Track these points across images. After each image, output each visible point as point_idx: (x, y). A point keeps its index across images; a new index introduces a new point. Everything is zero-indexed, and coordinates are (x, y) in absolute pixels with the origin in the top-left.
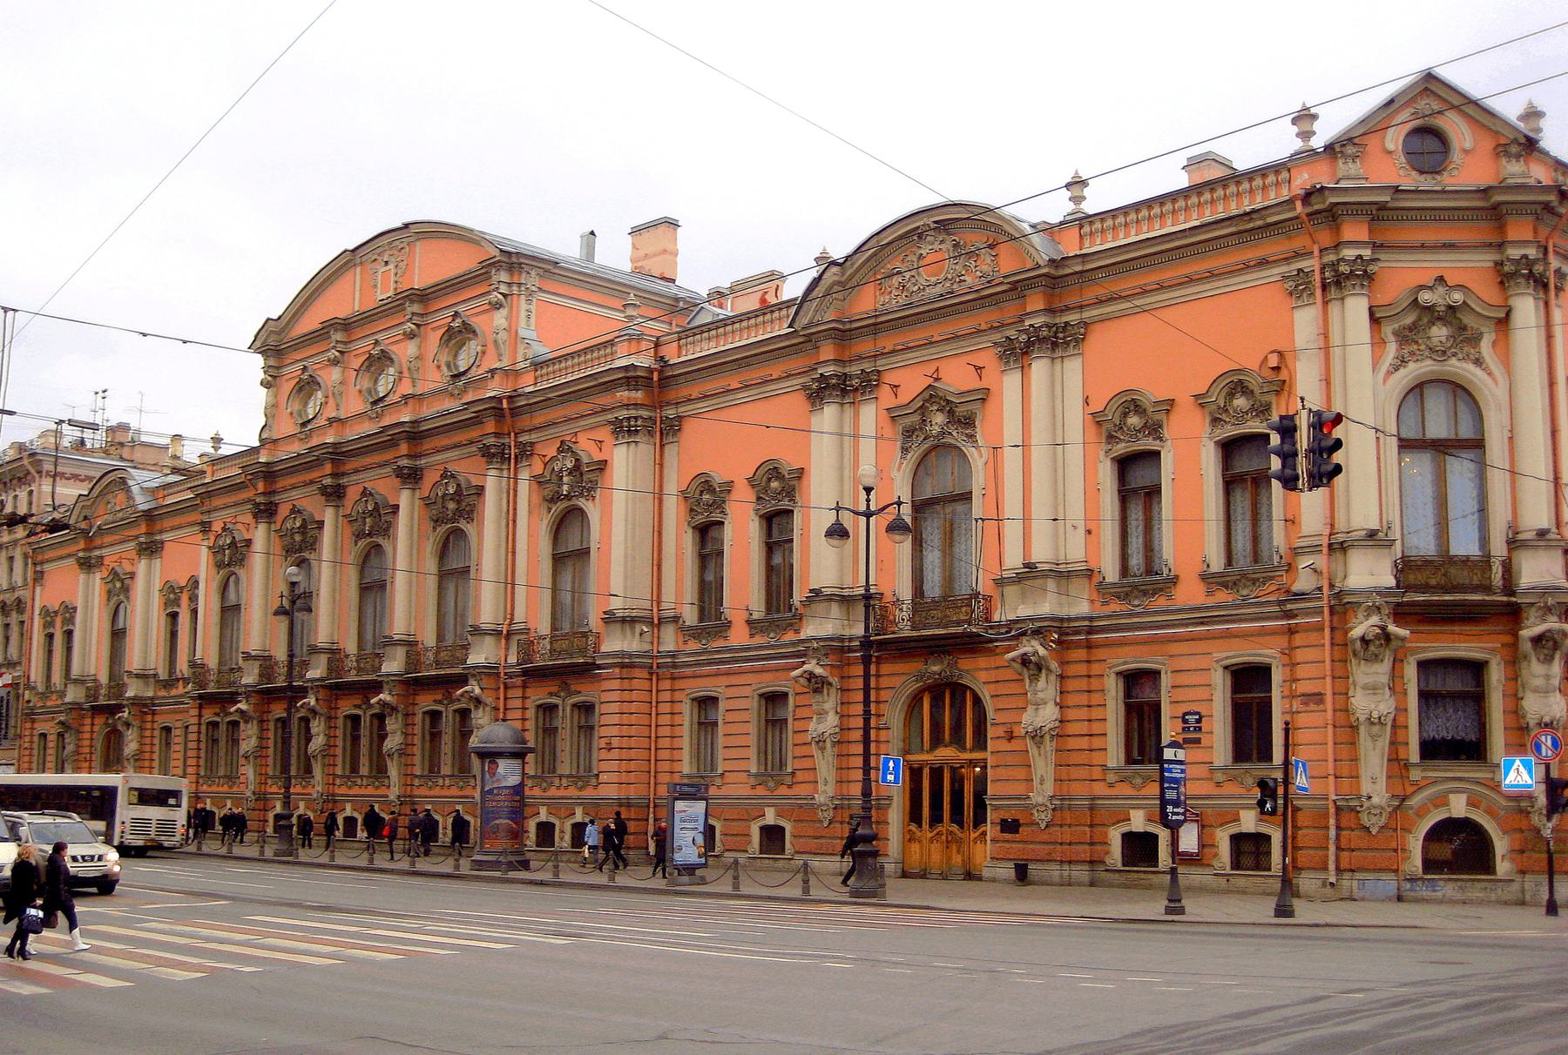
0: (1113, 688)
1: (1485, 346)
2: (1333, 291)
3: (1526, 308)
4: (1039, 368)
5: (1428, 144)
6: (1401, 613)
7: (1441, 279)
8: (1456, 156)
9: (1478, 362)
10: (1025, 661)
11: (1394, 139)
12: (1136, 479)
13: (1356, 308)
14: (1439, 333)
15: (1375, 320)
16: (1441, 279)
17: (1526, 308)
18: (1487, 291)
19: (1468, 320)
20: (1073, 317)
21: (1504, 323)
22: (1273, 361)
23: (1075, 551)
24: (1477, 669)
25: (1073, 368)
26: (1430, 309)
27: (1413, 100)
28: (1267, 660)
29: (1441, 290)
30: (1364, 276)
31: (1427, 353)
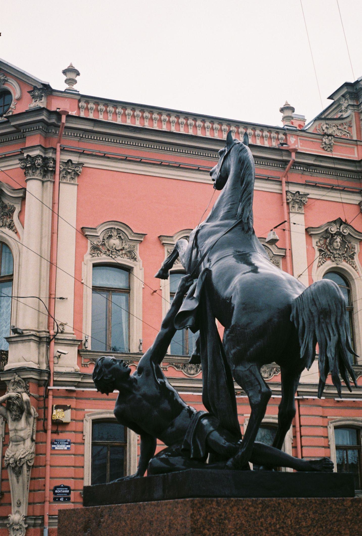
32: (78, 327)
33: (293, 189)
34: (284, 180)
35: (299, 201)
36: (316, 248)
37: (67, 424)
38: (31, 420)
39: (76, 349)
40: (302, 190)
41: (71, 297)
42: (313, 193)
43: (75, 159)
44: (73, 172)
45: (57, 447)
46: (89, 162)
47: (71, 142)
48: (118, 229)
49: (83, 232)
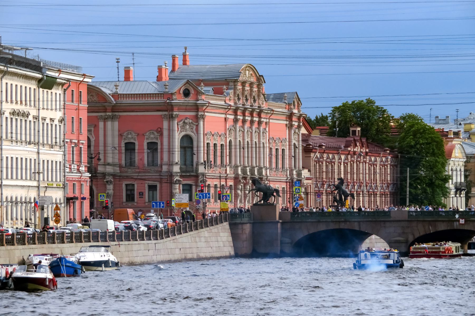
0: (124, 186)
2: (171, 119)
4: (109, 124)
6: (181, 176)
8: (191, 95)
10: (107, 182)
12: (130, 147)
15: (178, 125)
20: (117, 114)
21: (197, 126)
22: (159, 130)
23: (117, 161)
24: (190, 186)
25: (116, 124)
26: (186, 123)
27: (185, 84)
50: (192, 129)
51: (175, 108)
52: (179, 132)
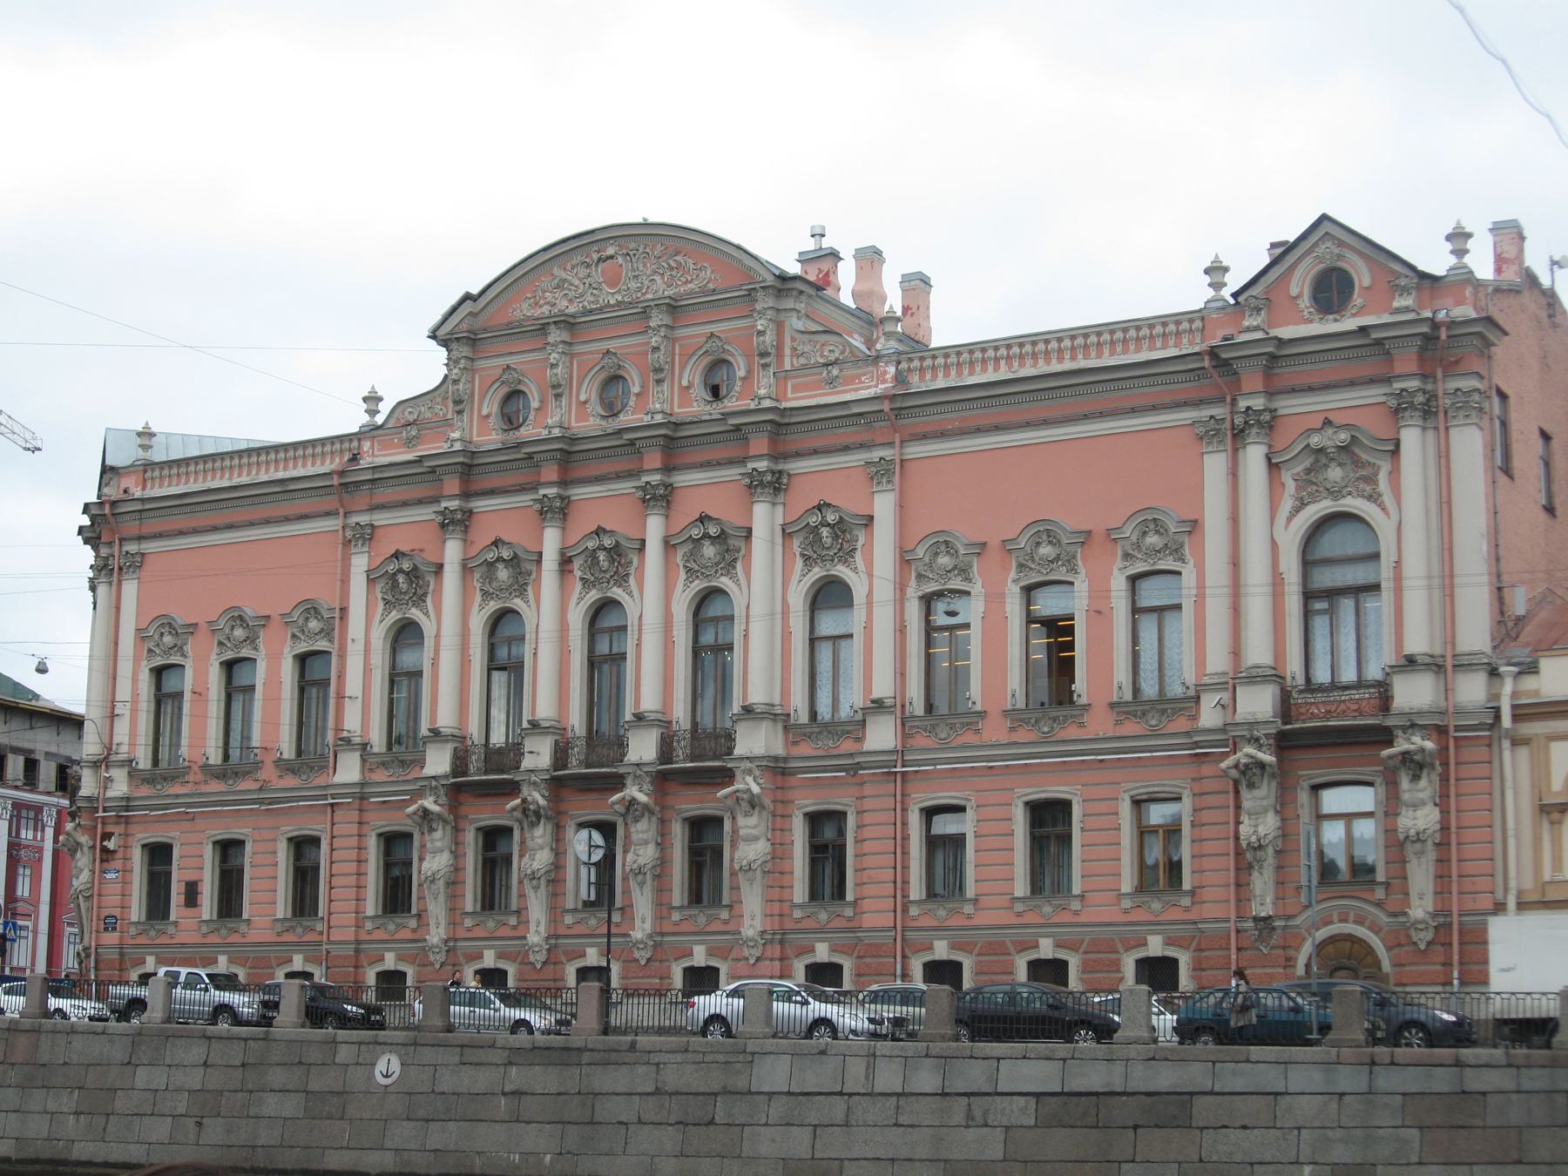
1: (1383, 478)
3: (1412, 438)
5: (1332, 290)
7: (1327, 423)
9: (1374, 497)
11: (1300, 284)
13: (1254, 455)
14: (1335, 473)
16: (1327, 423)
17: (1412, 438)
18: (1382, 428)
19: (1364, 456)
28: (1067, 796)
29: (1330, 431)
30: (1268, 423)
31: (1325, 494)
32: (132, 744)
33: (353, 520)
34: (341, 511)
35: (368, 535)
36: (380, 596)
37: (114, 852)
38: (86, 849)
39: (126, 770)
40: (363, 519)
41: (127, 713)
42: (380, 519)
43: (132, 547)
44: (136, 563)
45: (108, 876)
46: (148, 547)
47: (131, 527)
48: (169, 625)
49: (141, 635)
50: (1371, 480)
51: (1252, 379)
52: (1287, 504)
